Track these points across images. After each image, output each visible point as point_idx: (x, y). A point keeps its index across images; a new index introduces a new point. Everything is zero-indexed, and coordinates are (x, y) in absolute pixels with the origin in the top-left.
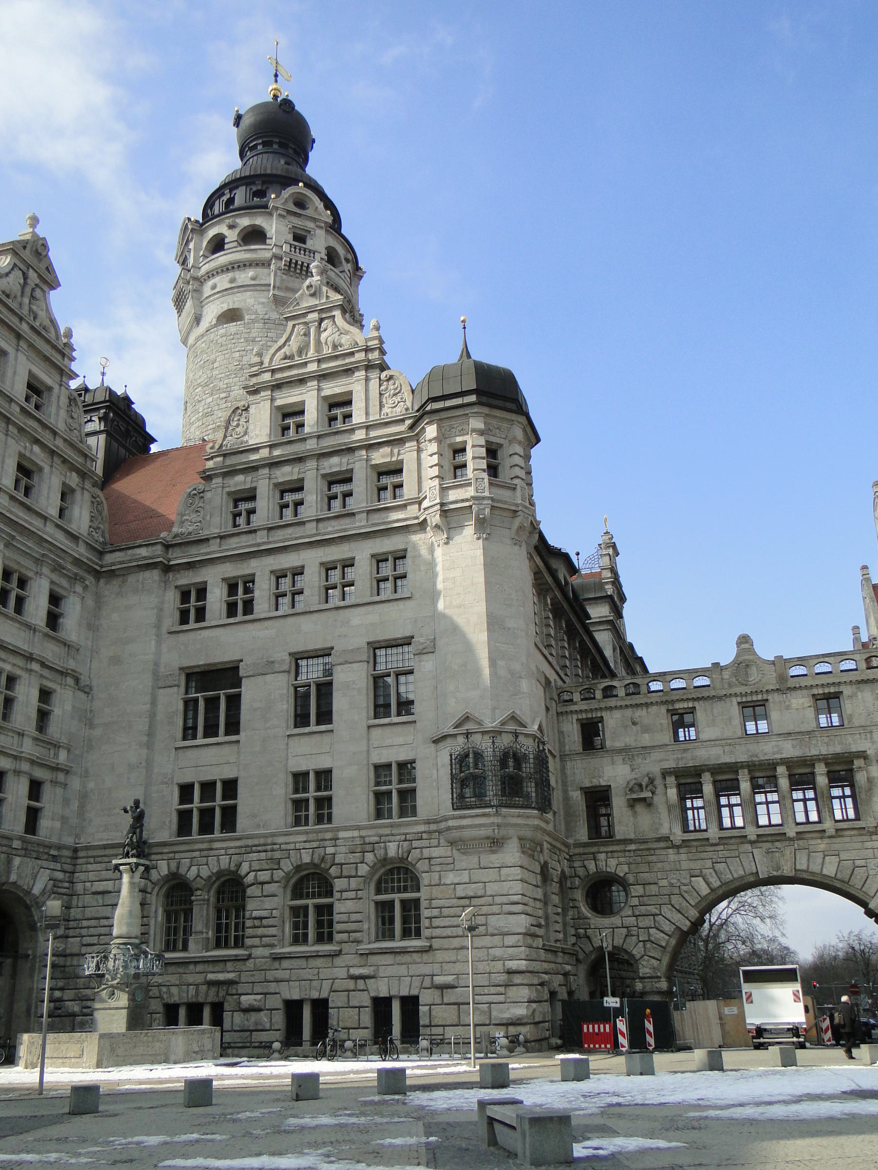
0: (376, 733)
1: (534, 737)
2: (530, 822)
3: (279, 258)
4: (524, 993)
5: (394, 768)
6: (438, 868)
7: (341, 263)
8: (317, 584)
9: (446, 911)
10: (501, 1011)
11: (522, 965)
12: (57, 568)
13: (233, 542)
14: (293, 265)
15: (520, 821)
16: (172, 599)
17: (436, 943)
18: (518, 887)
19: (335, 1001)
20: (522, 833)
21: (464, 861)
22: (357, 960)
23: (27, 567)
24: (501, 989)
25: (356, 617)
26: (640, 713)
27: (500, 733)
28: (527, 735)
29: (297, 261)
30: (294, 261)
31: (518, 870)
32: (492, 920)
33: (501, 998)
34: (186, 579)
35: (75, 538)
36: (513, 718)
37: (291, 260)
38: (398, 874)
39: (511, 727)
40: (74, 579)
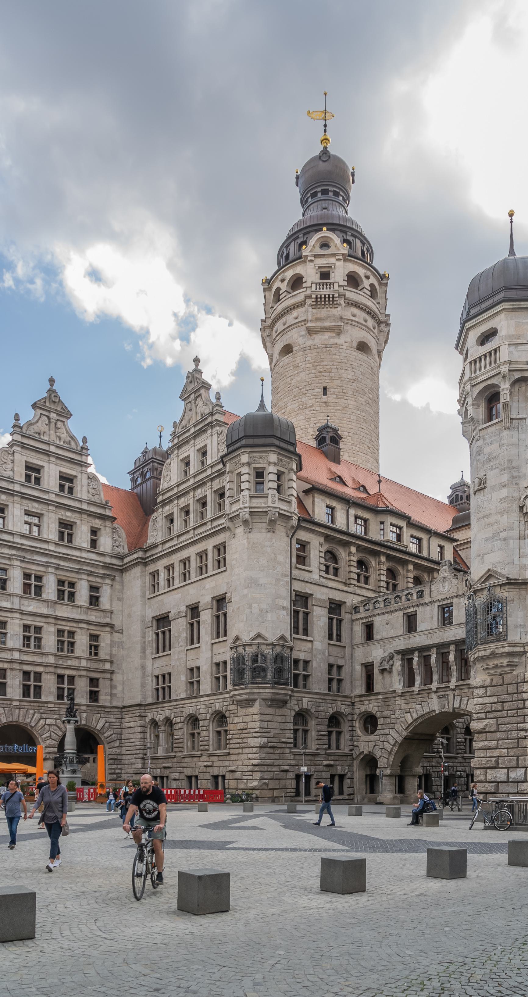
0: (215, 646)
1: (273, 645)
2: (267, 691)
3: (310, 297)
4: (257, 775)
5: (221, 664)
6: (232, 715)
7: (362, 281)
8: (194, 566)
9: (235, 736)
10: (251, 783)
11: (255, 762)
12: (90, 574)
13: (168, 545)
14: (319, 300)
15: (261, 691)
16: (148, 579)
17: (232, 751)
18: (258, 724)
19: (201, 776)
20: (264, 696)
21: (242, 712)
22: (207, 759)
23: (72, 576)
24: (251, 773)
25: (209, 584)
26: (391, 616)
27: (251, 645)
28: (267, 645)
29: (321, 296)
30: (319, 296)
31: (258, 716)
32: (249, 740)
33: (251, 777)
34: (152, 568)
35: (102, 555)
36: (259, 636)
37: (317, 296)
38: (221, 718)
39: (259, 640)
40: (104, 576)
